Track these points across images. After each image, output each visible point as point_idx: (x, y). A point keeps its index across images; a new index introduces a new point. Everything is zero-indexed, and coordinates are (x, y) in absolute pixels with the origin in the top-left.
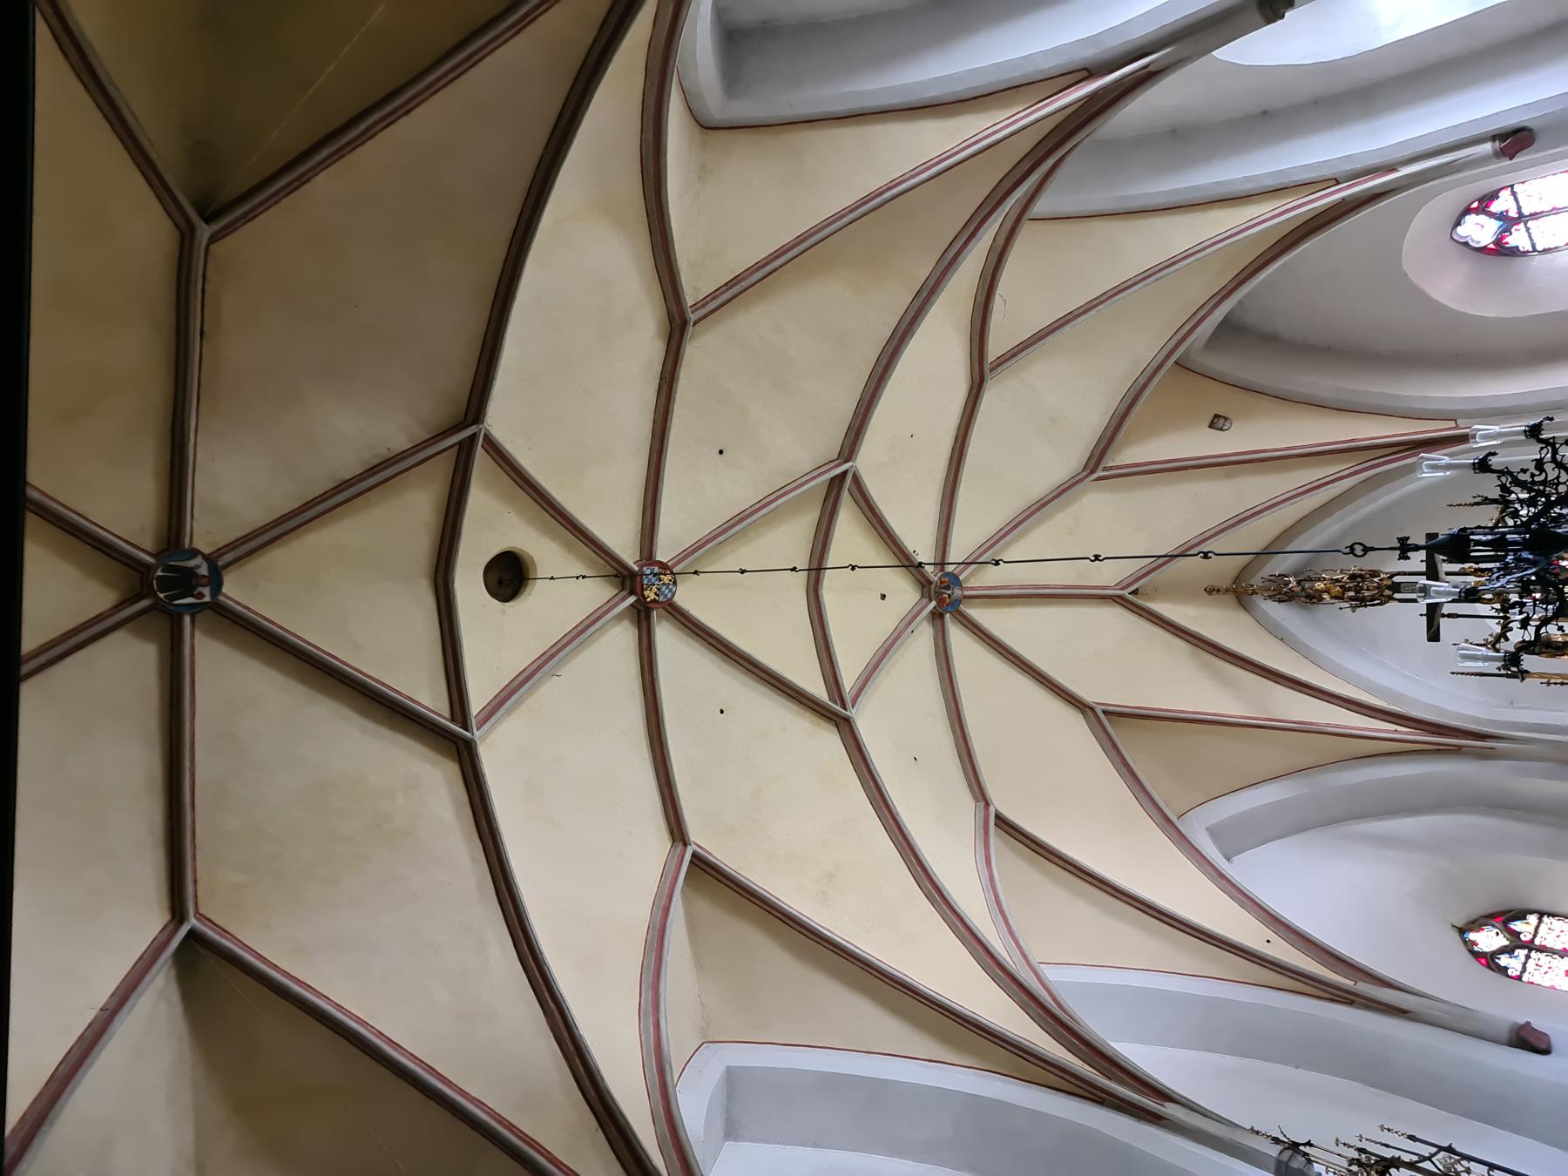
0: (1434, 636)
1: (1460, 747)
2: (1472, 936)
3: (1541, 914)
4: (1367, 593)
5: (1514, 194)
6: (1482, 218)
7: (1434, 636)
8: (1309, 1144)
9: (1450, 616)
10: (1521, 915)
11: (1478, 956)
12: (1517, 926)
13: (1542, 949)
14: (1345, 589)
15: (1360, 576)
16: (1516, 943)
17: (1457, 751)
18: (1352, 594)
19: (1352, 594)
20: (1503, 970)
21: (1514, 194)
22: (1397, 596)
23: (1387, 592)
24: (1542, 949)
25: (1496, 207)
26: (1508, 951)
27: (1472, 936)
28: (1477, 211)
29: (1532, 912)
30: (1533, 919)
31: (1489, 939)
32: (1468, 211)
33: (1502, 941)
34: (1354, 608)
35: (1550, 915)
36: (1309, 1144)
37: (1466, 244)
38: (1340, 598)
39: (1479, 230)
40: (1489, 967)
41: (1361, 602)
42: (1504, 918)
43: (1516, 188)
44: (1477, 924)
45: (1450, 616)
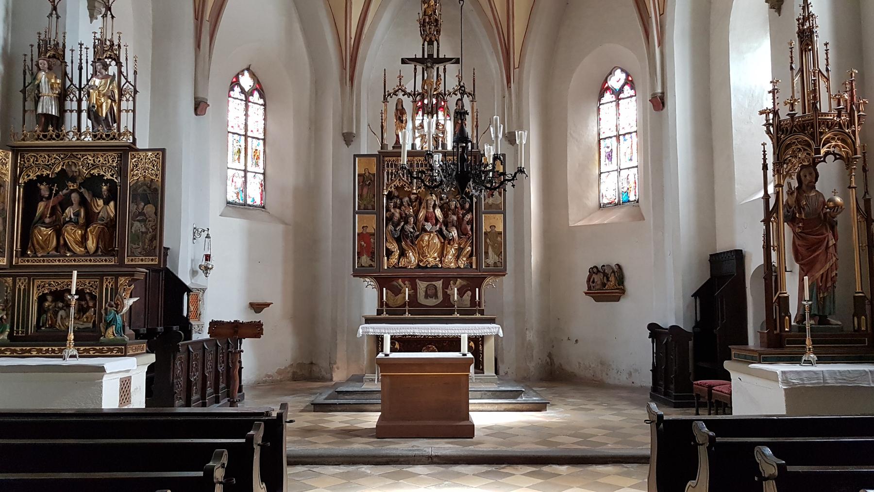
0: (404, 61)
1: (345, 69)
2: (246, 73)
3: (264, 105)
4: (428, 27)
5: (631, 97)
6: (622, 82)
7: (404, 61)
8: (113, 17)
9: (415, 69)
10: (262, 96)
11: (237, 77)
12: (256, 94)
13: (247, 106)
14: (430, 16)
15: (436, 26)
16: (247, 95)
17: (344, 68)
18: (427, 20)
19: (427, 20)
20: (232, 89)
21: (631, 97)
22: (426, 43)
23: (428, 39)
24: (247, 106)
25: (627, 88)
26: (243, 91)
27: (246, 73)
28: (627, 79)
29: (265, 101)
30: (261, 101)
31: (246, 81)
32: (628, 75)
33: (247, 89)
34: (419, 21)
35: (265, 109)
36: (113, 17)
37: (611, 74)
38: (425, 14)
39: (617, 80)
40: (232, 83)
41: (423, 25)
42: (259, 88)
43: (634, 98)
44: (253, 75)
45: (415, 69)
